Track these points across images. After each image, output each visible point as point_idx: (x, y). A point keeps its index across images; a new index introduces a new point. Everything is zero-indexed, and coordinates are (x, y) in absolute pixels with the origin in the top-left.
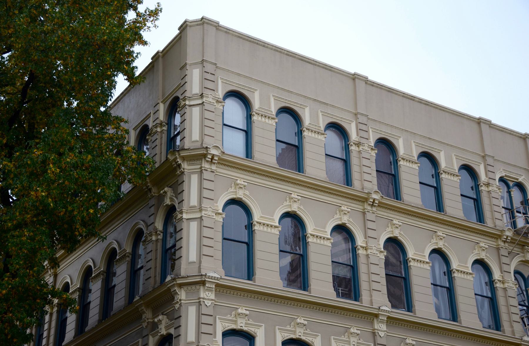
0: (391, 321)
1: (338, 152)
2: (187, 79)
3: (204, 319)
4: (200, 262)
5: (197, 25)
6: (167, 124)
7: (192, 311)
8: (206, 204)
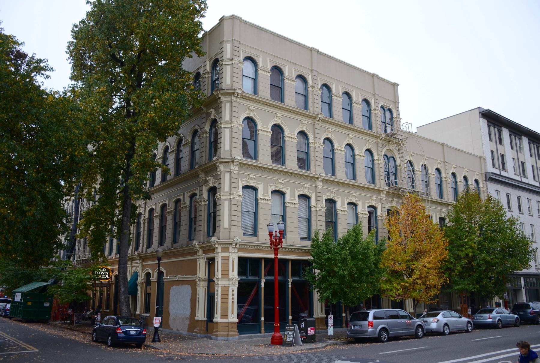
0: (325, 181)
1: (302, 91)
2: (224, 49)
3: (233, 180)
4: (231, 151)
5: (230, 19)
6: (211, 73)
7: (227, 176)
8: (234, 120)
